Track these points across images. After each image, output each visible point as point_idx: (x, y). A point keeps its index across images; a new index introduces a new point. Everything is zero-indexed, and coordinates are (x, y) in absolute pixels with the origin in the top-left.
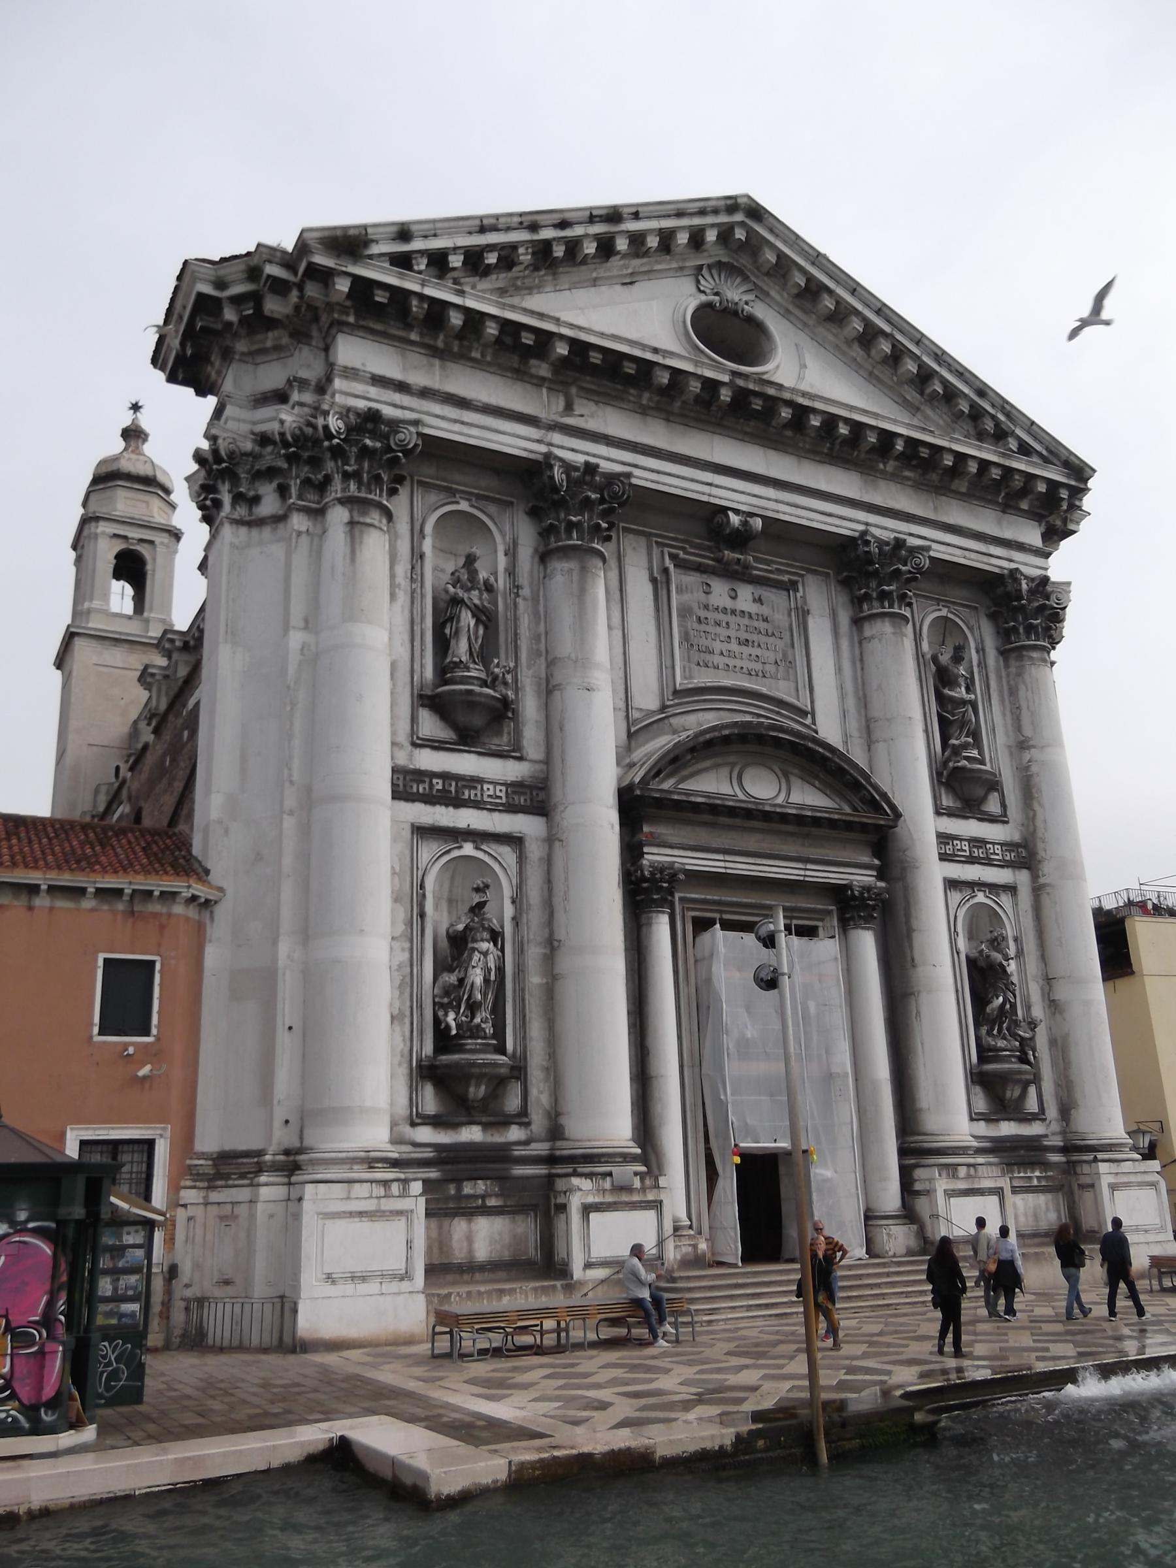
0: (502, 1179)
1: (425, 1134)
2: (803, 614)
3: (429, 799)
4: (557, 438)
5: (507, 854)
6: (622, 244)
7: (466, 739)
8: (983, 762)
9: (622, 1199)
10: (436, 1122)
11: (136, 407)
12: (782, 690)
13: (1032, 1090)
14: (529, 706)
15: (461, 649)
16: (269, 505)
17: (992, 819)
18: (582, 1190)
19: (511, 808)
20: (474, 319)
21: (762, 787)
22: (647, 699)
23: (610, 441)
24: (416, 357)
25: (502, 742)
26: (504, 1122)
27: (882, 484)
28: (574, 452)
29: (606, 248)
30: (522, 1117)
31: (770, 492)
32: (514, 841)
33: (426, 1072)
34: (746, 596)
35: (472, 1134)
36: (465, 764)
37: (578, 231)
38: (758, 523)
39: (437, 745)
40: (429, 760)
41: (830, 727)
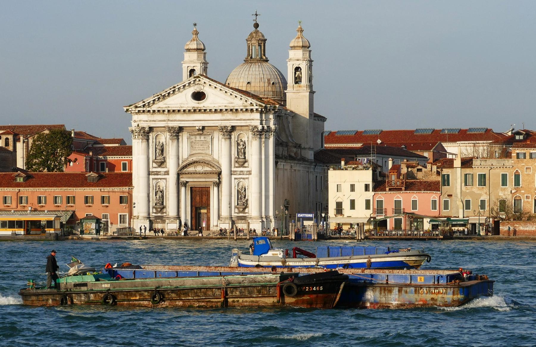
0: (162, 219)
1: (154, 214)
2: (212, 139)
3: (154, 175)
4: (169, 122)
5: (164, 181)
6: (177, 90)
7: (159, 166)
8: (245, 158)
9: (172, 222)
10: (155, 213)
11: (195, 25)
12: (207, 152)
13: (247, 209)
14: (168, 160)
15: (157, 154)
16: (136, 137)
17: (245, 167)
18: (167, 221)
19: (165, 175)
20: (154, 111)
21: (199, 169)
22: (185, 156)
23: (177, 120)
24: (150, 115)
25: (164, 166)
26: (163, 213)
27: (226, 115)
28: (171, 124)
29: (174, 91)
30: (166, 213)
31: (203, 122)
32: (165, 179)
33: (153, 207)
34: (202, 137)
35: (159, 214)
36: (159, 169)
37: (168, 92)
38: (201, 128)
39: (155, 167)
40: (154, 170)
41: (216, 156)
